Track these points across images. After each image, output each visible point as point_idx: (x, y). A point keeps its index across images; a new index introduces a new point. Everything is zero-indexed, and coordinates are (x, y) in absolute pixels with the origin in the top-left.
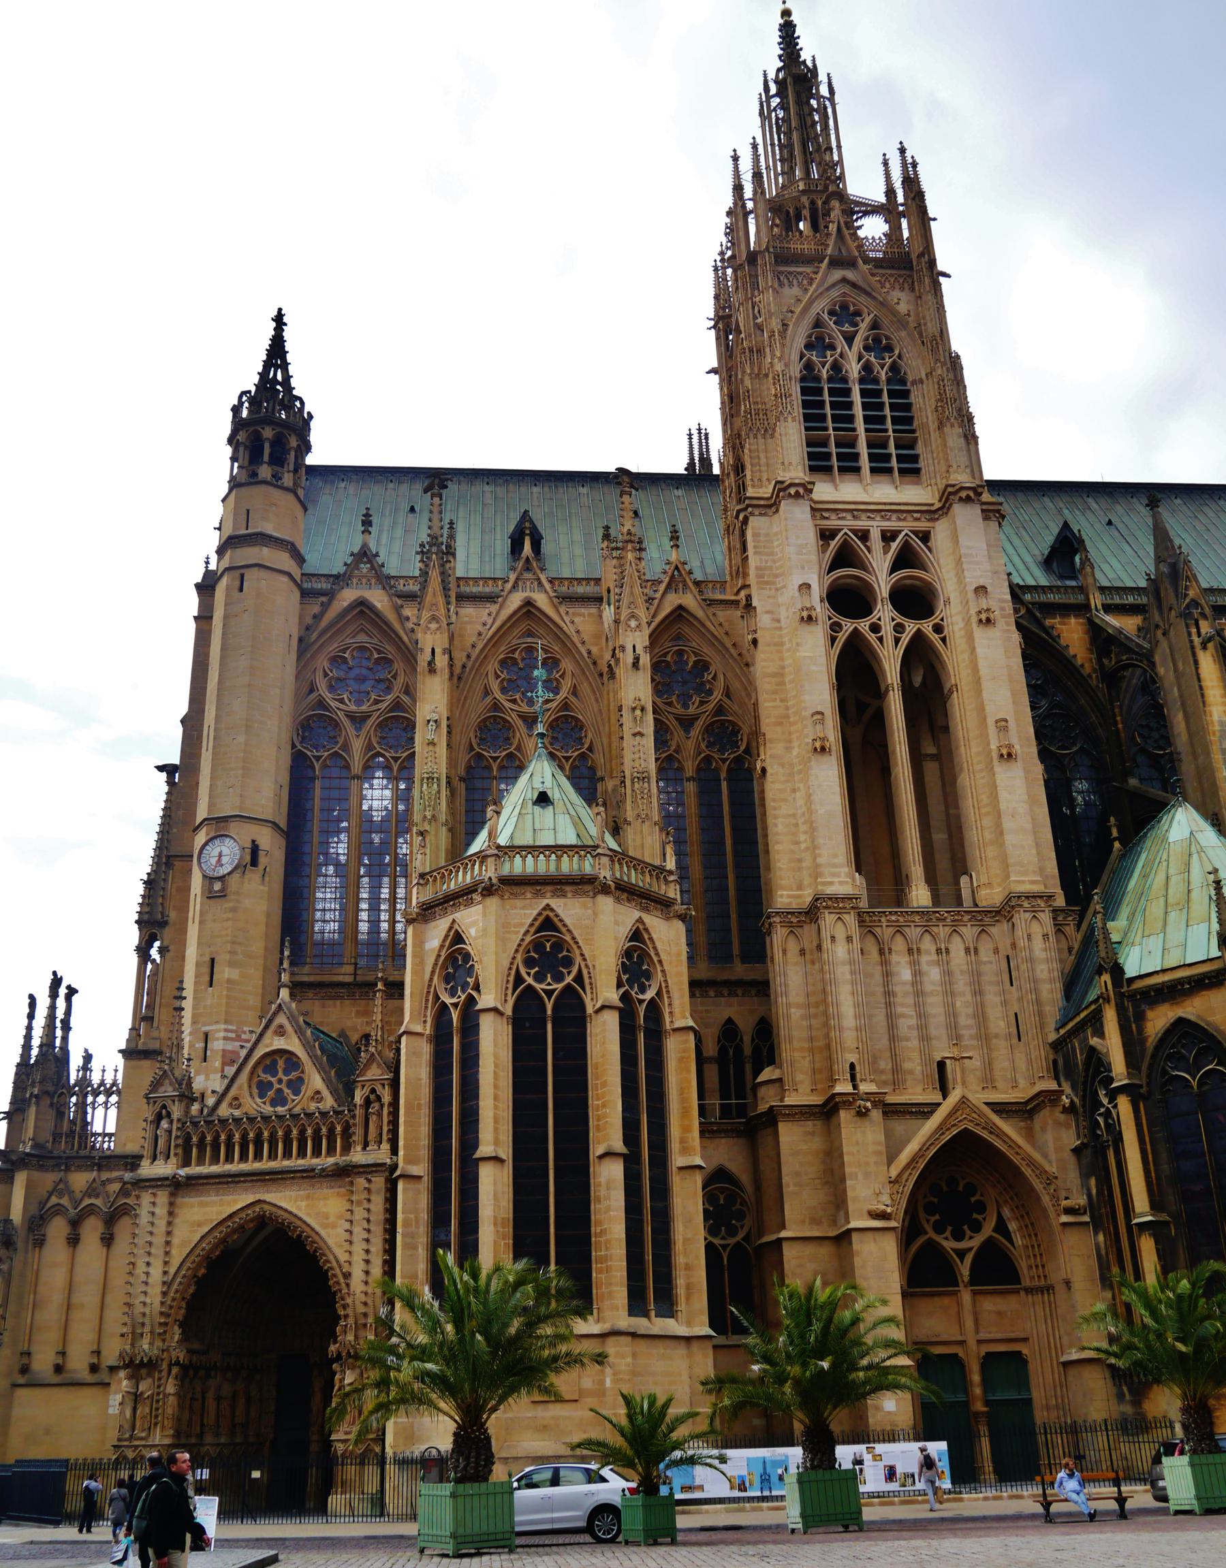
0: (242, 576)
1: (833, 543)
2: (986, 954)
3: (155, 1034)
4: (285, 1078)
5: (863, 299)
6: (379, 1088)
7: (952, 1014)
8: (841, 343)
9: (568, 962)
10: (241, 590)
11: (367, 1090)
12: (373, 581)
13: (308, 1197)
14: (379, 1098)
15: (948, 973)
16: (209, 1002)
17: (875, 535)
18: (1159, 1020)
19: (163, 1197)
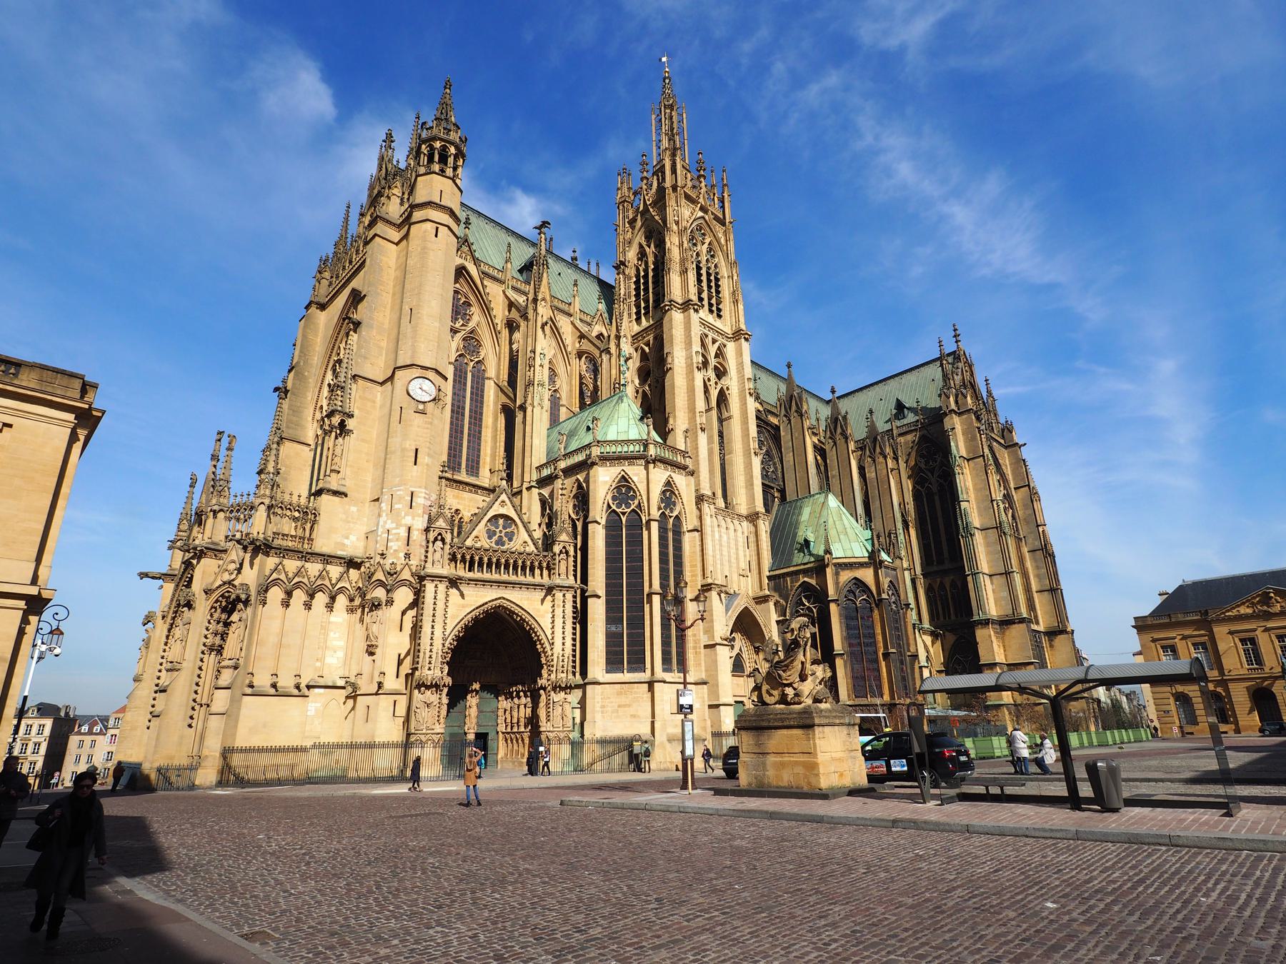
0: (437, 228)
2: (739, 534)
3: (343, 482)
4: (498, 530)
5: (708, 229)
6: (568, 548)
7: (730, 556)
8: (699, 244)
9: (674, 504)
10: (436, 236)
11: (561, 546)
12: (469, 257)
13: (528, 599)
14: (567, 553)
15: (729, 538)
16: (414, 474)
17: (710, 338)
18: (846, 576)
19: (442, 587)
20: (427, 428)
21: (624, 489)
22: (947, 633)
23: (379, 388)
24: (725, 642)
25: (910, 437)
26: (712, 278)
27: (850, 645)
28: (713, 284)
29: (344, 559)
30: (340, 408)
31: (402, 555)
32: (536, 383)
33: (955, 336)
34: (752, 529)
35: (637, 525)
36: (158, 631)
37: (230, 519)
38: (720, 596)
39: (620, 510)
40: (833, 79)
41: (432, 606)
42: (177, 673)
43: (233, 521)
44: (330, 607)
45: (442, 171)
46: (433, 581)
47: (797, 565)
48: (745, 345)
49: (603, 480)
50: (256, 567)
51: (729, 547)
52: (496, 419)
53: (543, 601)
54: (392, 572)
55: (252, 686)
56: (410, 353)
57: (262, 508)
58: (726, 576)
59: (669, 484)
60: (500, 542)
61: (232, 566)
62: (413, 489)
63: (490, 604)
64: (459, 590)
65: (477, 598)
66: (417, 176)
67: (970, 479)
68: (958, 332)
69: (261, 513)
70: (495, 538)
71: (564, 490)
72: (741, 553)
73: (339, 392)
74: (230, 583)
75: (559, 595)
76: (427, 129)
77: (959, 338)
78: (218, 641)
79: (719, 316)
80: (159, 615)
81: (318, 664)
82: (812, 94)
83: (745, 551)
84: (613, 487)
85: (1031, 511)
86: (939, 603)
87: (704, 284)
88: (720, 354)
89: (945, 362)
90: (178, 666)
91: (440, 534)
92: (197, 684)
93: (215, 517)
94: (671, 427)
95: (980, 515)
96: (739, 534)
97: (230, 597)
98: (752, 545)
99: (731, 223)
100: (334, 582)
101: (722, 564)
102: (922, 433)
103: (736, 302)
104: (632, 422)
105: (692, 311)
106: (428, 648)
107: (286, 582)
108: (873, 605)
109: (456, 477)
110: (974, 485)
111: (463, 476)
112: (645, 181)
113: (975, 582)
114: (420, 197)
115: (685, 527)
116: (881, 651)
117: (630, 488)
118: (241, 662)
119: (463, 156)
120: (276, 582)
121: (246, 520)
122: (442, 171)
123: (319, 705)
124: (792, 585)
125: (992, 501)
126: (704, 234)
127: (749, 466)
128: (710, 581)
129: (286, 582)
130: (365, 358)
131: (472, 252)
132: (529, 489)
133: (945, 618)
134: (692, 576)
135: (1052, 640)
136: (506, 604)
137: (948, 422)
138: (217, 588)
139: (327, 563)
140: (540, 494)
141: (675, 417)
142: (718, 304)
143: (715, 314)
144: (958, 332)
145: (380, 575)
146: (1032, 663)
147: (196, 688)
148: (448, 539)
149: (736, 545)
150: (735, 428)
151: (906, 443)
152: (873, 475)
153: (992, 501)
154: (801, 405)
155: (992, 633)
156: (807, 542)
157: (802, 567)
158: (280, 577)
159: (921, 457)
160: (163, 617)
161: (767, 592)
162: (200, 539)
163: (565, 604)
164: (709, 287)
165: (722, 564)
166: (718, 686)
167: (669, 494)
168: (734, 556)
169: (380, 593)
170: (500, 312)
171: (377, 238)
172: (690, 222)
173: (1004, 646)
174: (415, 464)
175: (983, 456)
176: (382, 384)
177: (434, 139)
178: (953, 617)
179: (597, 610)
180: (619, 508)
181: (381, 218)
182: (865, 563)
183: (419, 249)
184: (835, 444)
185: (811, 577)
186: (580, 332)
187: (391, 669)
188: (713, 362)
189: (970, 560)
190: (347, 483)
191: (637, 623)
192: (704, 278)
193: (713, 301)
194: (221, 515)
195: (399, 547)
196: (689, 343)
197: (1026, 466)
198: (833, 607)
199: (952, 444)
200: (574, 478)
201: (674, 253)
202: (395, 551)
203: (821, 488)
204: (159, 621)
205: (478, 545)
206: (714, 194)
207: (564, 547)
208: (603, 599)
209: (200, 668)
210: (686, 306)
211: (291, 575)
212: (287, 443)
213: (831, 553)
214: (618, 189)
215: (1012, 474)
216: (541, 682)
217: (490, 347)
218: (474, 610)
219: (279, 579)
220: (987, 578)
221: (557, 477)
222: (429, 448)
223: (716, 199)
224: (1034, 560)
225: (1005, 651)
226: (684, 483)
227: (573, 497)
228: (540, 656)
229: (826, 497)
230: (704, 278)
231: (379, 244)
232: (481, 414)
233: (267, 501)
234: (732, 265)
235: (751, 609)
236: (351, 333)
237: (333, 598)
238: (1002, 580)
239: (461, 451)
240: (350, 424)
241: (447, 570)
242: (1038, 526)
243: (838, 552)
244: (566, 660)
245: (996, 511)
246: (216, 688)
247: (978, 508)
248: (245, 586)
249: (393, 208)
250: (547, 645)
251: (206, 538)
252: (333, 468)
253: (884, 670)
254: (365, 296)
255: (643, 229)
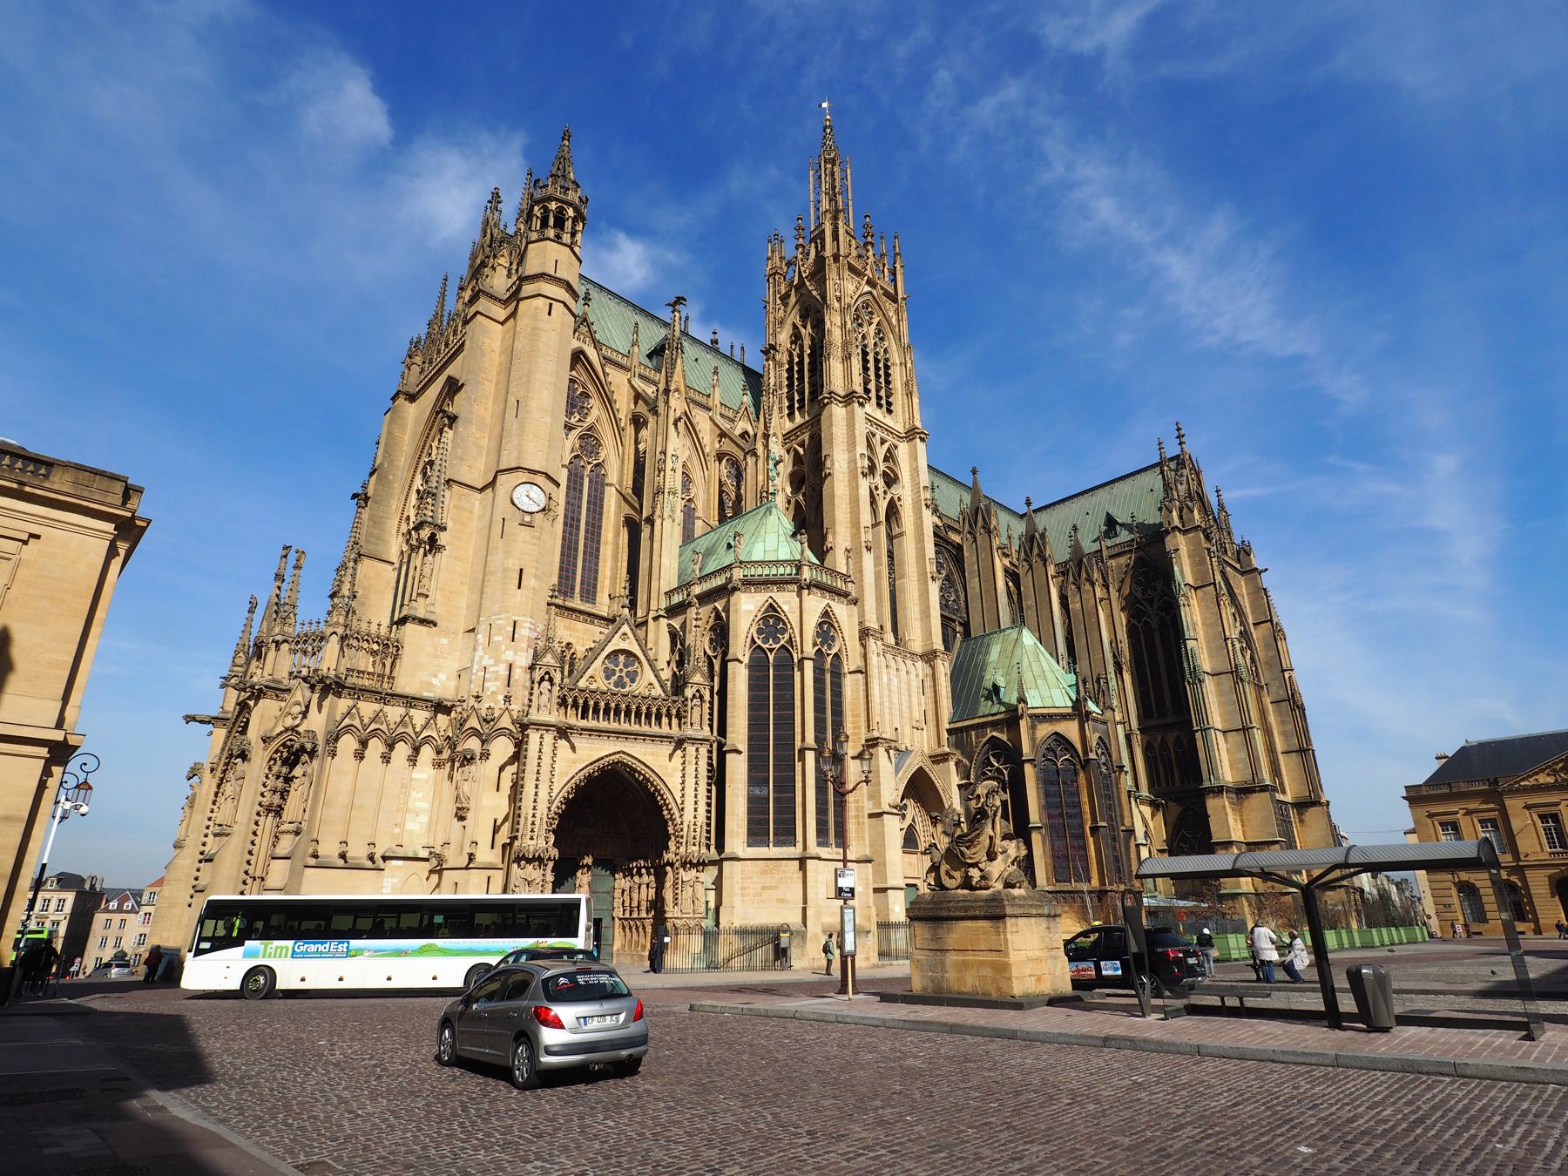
0: (551, 305)
2: (913, 676)
3: (432, 608)
4: (617, 669)
5: (876, 307)
7: (900, 704)
10: (549, 314)
11: (694, 689)
13: (653, 754)
14: (701, 697)
16: (518, 599)
18: (1044, 730)
19: (549, 738)
20: (535, 544)
21: (772, 620)
22: (1170, 803)
23: (477, 495)
24: (895, 811)
25: (1123, 560)
26: (881, 365)
27: (1050, 816)
28: (882, 373)
29: (431, 701)
30: (430, 520)
31: (501, 698)
32: (666, 490)
33: (1178, 437)
34: (929, 670)
35: (787, 665)
36: (205, 787)
37: (295, 652)
38: (888, 753)
39: (767, 646)
40: (1012, 91)
41: (536, 761)
42: (227, 838)
43: (299, 654)
44: (413, 760)
45: (558, 237)
46: (537, 730)
47: (983, 716)
48: (921, 447)
49: (746, 608)
50: (325, 710)
51: (900, 693)
52: (617, 535)
53: (671, 756)
54: (489, 718)
55: (316, 857)
56: (515, 454)
57: (334, 639)
58: (896, 729)
59: (826, 614)
60: (620, 683)
61: (297, 709)
62: (516, 618)
63: (607, 759)
64: (569, 741)
65: (591, 752)
66: (528, 243)
67: (1198, 613)
68: (1182, 432)
69: (333, 645)
70: (615, 678)
71: (698, 621)
72: (915, 700)
73: (429, 500)
74: (293, 729)
75: (691, 749)
76: (541, 188)
77: (1183, 440)
78: (276, 800)
79: (890, 411)
80: (207, 767)
81: (397, 830)
82: (986, 110)
83: (919, 698)
84: (759, 617)
85: (1274, 653)
86: (1160, 765)
87: (872, 373)
88: (890, 456)
89: (1166, 468)
90: (228, 830)
91: (547, 673)
92: (250, 853)
93: (277, 649)
94: (829, 546)
95: (1211, 656)
96: (913, 676)
97: (292, 746)
98: (929, 691)
99: (904, 299)
100: (418, 729)
101: (891, 714)
102: (1138, 555)
103: (909, 394)
104: (782, 538)
105: (856, 405)
106: (531, 812)
107: (360, 728)
108: (1078, 767)
109: (568, 604)
110: (1204, 620)
111: (576, 603)
112: (801, 250)
113: (1205, 739)
114: (531, 267)
115: (846, 667)
116: (1088, 824)
117: (779, 619)
118: (304, 826)
119: (583, 220)
120: (349, 729)
121: (314, 654)
122: (558, 237)
123: (396, 880)
124: (978, 741)
125: (1226, 639)
126: (871, 313)
127: (924, 594)
128: (876, 734)
129: (360, 728)
130: (461, 459)
131: (592, 334)
132: (656, 619)
133: (1167, 784)
134: (855, 728)
135: (1302, 814)
136: (626, 759)
137: (1170, 543)
138: (278, 735)
139: (411, 707)
140: (669, 625)
141: (834, 533)
142: (887, 397)
143: (884, 409)
144: (1182, 432)
145: (473, 722)
146: (1277, 842)
147: (249, 857)
148: (557, 680)
149: (909, 691)
150: (908, 547)
151: (1119, 567)
152: (1079, 605)
153: (1226, 639)
154: (990, 519)
155: (1227, 804)
156: (996, 688)
157: (990, 718)
158: (354, 723)
159: (1136, 583)
160: (212, 770)
161: (947, 749)
162: (259, 675)
163: (698, 761)
164: (878, 376)
165: (891, 714)
166: (885, 864)
167: (827, 626)
168: (905, 704)
169: (473, 744)
170: (624, 404)
171: (479, 316)
172: (855, 298)
173: (1242, 821)
174: (519, 588)
175: (1214, 584)
176: (481, 490)
177: (550, 199)
178: (1178, 783)
179: (738, 768)
180: (765, 643)
181: (483, 292)
182: (1069, 714)
183: (529, 329)
184: (1031, 567)
185: (1002, 732)
186: (720, 429)
187: (485, 838)
188: (881, 467)
189: (1198, 712)
190: (437, 609)
191: (786, 785)
192: (871, 365)
193: (882, 393)
194: (285, 647)
195: (498, 688)
196: (852, 444)
197: (1267, 597)
198: (1028, 768)
199: (1176, 568)
200: (711, 606)
201: (835, 335)
202: (492, 692)
203: (1013, 622)
204: (207, 775)
205: (593, 687)
206: (884, 265)
207: (698, 691)
208: (745, 755)
209: (255, 834)
210: (849, 398)
211: (366, 721)
212: (366, 561)
213: (1025, 702)
214: (768, 259)
215: (1251, 606)
216: (667, 857)
217: (611, 447)
218: (587, 766)
219: (352, 725)
220: (1220, 735)
221: (690, 605)
222: (536, 568)
223: (886, 270)
224: (1279, 713)
225: (1243, 826)
226: (845, 613)
227: (710, 630)
228: (667, 826)
229: (1020, 632)
230: (871, 365)
231: (481, 323)
232: (600, 527)
233: (340, 631)
234: (905, 349)
235: (927, 770)
236: (446, 429)
237: (417, 750)
238: (1239, 737)
239: (574, 573)
240: (442, 538)
241: (554, 717)
242: (1283, 671)
243: (1034, 700)
244: (698, 830)
245: (1231, 652)
246: (273, 858)
247: (1209, 649)
248: (312, 734)
249: (499, 281)
250: (675, 810)
251: (265, 674)
252: (420, 591)
253: (1092, 847)
254: (463, 385)
255: (797, 307)
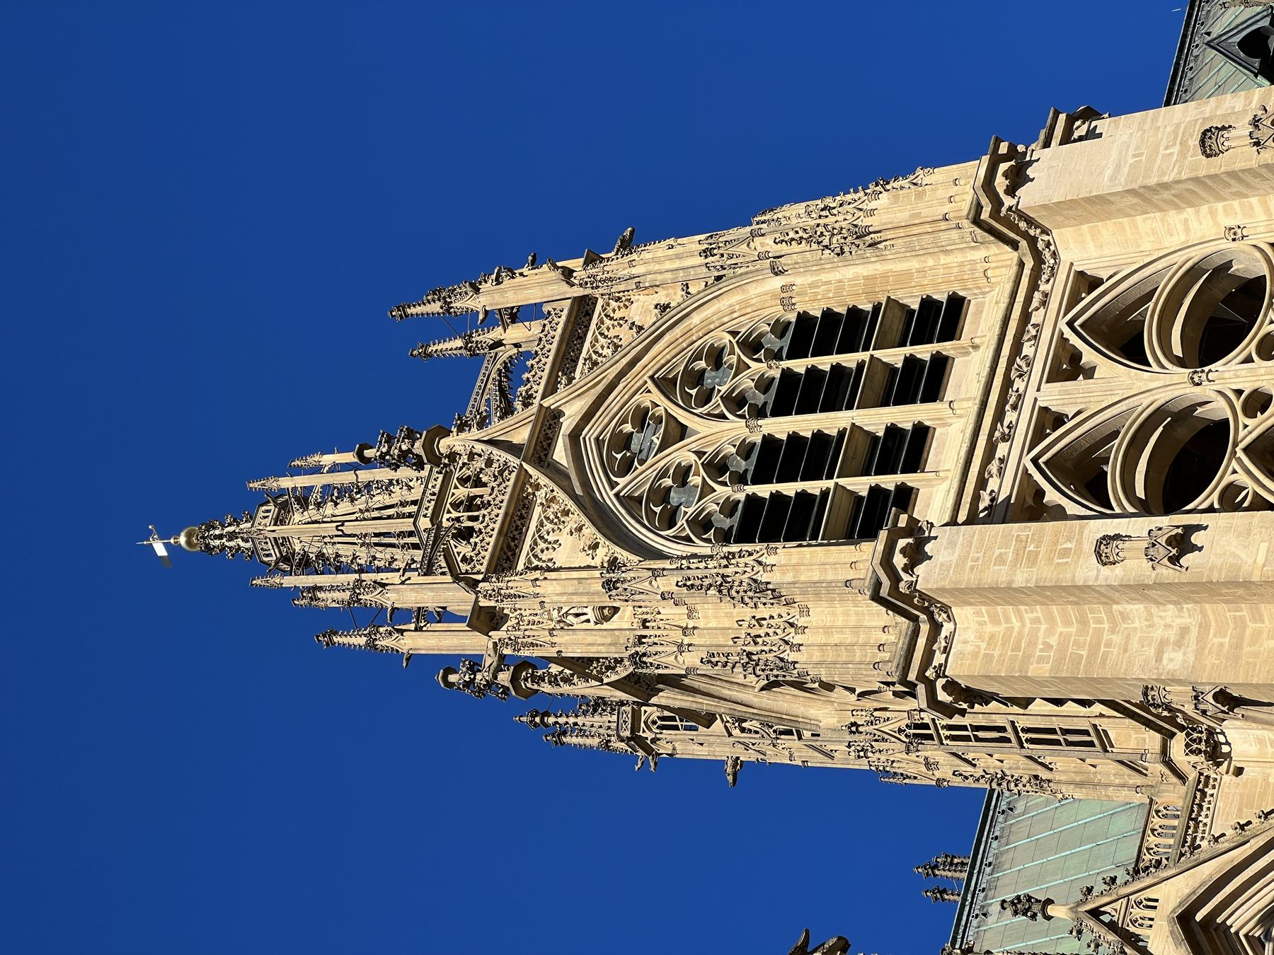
1: (1052, 496)
5: (614, 401)
17: (1057, 396)
87: (831, 422)
192: (806, 424)
206: (499, 344)
230: (806, 424)
